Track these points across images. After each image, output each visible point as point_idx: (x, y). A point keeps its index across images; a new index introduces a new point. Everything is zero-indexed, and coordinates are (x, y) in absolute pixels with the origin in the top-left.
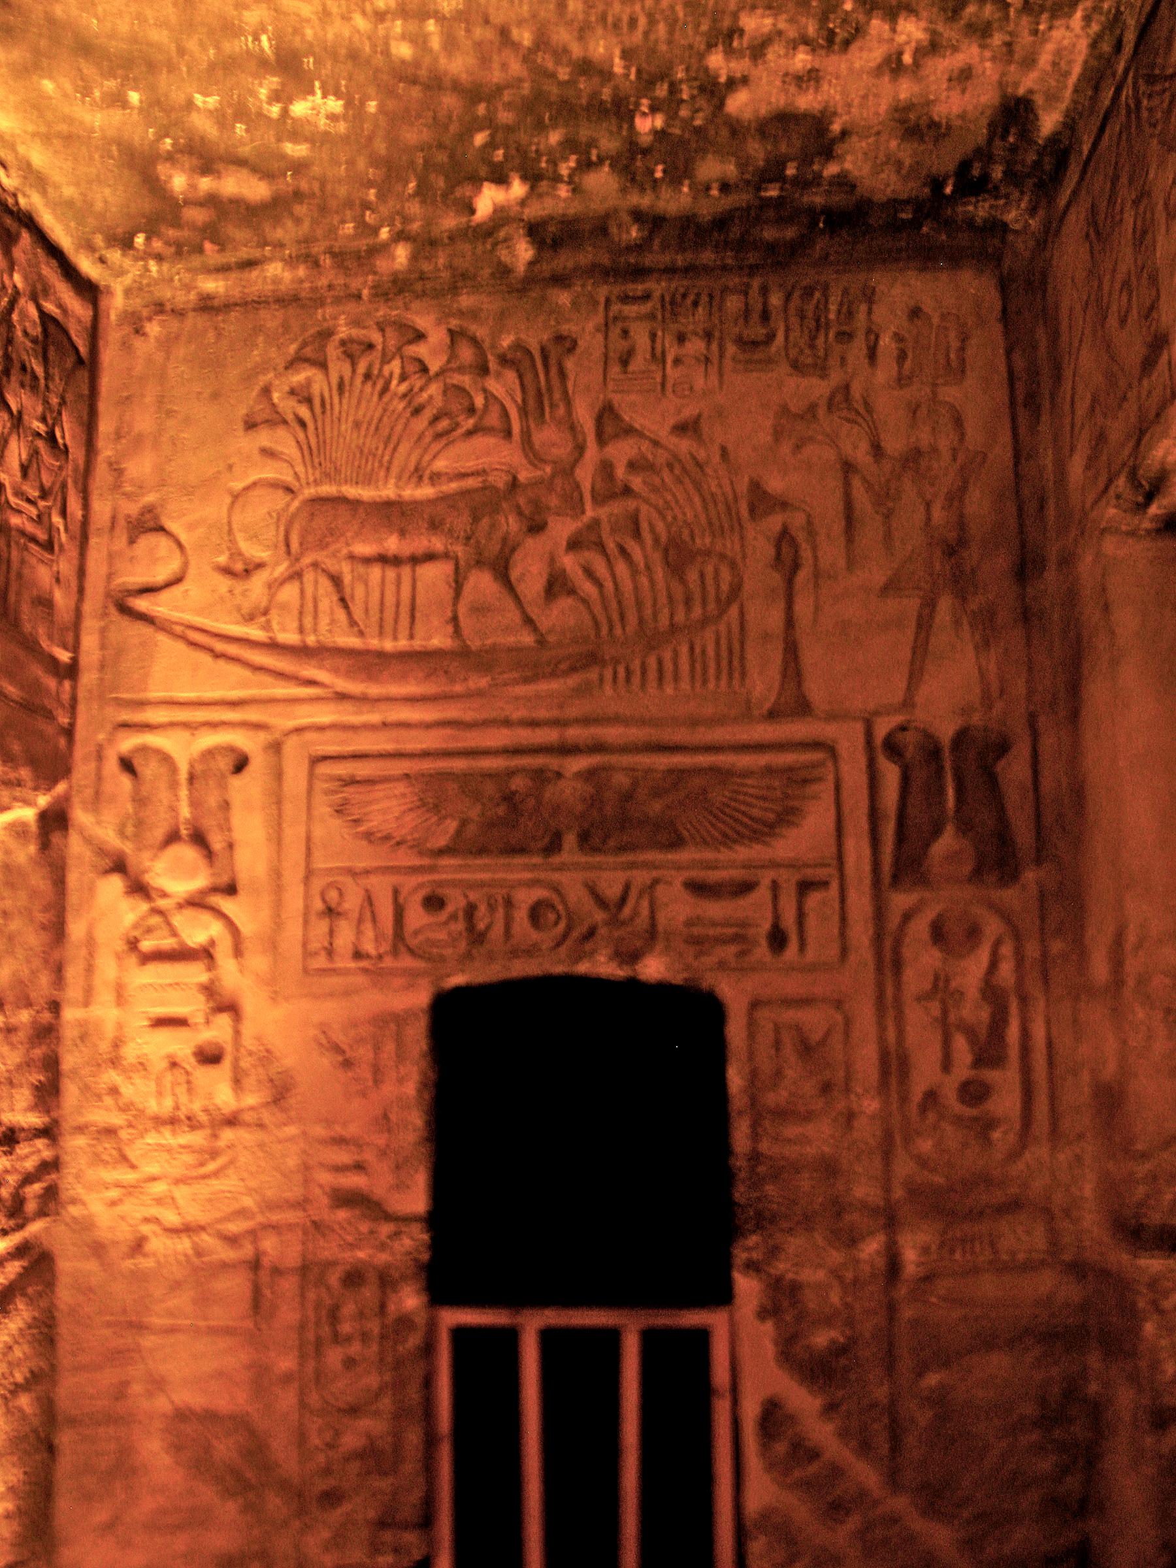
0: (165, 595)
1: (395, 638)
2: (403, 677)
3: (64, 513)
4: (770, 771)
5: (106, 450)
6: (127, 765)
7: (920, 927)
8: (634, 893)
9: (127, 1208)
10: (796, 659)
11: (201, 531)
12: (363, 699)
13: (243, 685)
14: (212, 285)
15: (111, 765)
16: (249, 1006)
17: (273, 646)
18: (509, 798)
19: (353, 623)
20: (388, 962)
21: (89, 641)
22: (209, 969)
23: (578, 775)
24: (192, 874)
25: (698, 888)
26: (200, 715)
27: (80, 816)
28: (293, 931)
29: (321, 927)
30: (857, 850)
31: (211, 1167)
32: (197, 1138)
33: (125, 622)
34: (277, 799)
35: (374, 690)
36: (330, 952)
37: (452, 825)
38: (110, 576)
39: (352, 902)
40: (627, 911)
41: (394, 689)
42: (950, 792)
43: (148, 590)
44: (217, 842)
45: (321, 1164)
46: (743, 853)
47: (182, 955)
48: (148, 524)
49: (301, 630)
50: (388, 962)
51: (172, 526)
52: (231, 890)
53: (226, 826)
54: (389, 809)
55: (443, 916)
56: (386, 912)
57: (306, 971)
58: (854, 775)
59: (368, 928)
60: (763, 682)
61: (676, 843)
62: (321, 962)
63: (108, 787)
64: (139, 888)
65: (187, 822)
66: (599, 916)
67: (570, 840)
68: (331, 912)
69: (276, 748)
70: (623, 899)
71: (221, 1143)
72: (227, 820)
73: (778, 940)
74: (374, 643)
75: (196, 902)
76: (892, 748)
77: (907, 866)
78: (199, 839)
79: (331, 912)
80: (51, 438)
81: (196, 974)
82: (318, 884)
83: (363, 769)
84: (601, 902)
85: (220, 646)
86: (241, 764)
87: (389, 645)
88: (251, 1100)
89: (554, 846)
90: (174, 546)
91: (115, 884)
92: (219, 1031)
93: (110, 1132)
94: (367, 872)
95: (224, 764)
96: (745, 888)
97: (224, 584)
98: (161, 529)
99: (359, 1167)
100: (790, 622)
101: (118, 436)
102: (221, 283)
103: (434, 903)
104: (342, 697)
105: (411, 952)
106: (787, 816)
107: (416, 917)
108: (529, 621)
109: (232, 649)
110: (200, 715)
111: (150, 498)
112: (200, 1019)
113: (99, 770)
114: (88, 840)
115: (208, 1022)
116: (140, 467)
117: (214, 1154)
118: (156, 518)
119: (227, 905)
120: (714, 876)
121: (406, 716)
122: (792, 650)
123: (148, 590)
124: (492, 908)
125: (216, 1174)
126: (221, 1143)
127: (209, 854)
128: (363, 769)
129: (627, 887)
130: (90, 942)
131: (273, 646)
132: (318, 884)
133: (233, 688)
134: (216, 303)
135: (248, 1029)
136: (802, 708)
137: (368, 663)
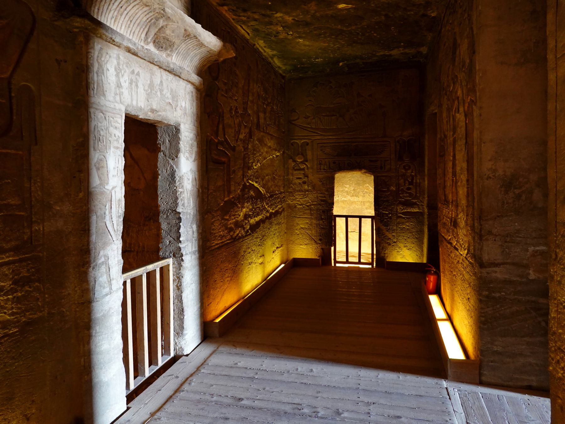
9: (294, 202)
16: (309, 176)
17: (312, 128)
26: (301, 138)
28: (316, 166)
32: (303, 193)
36: (320, 169)
47: (300, 169)
52: (307, 161)
64: (294, 161)
68: (320, 164)
73: (381, 168)
75: (302, 162)
78: (302, 154)
79: (320, 164)
83: (325, 145)
86: (308, 144)
91: (290, 161)
92: (306, 179)
93: (291, 192)
99: (325, 197)
103: (334, 163)
110: (301, 138)
127: (304, 157)
128: (325, 145)
130: (288, 168)
131: (312, 128)
135: (309, 179)
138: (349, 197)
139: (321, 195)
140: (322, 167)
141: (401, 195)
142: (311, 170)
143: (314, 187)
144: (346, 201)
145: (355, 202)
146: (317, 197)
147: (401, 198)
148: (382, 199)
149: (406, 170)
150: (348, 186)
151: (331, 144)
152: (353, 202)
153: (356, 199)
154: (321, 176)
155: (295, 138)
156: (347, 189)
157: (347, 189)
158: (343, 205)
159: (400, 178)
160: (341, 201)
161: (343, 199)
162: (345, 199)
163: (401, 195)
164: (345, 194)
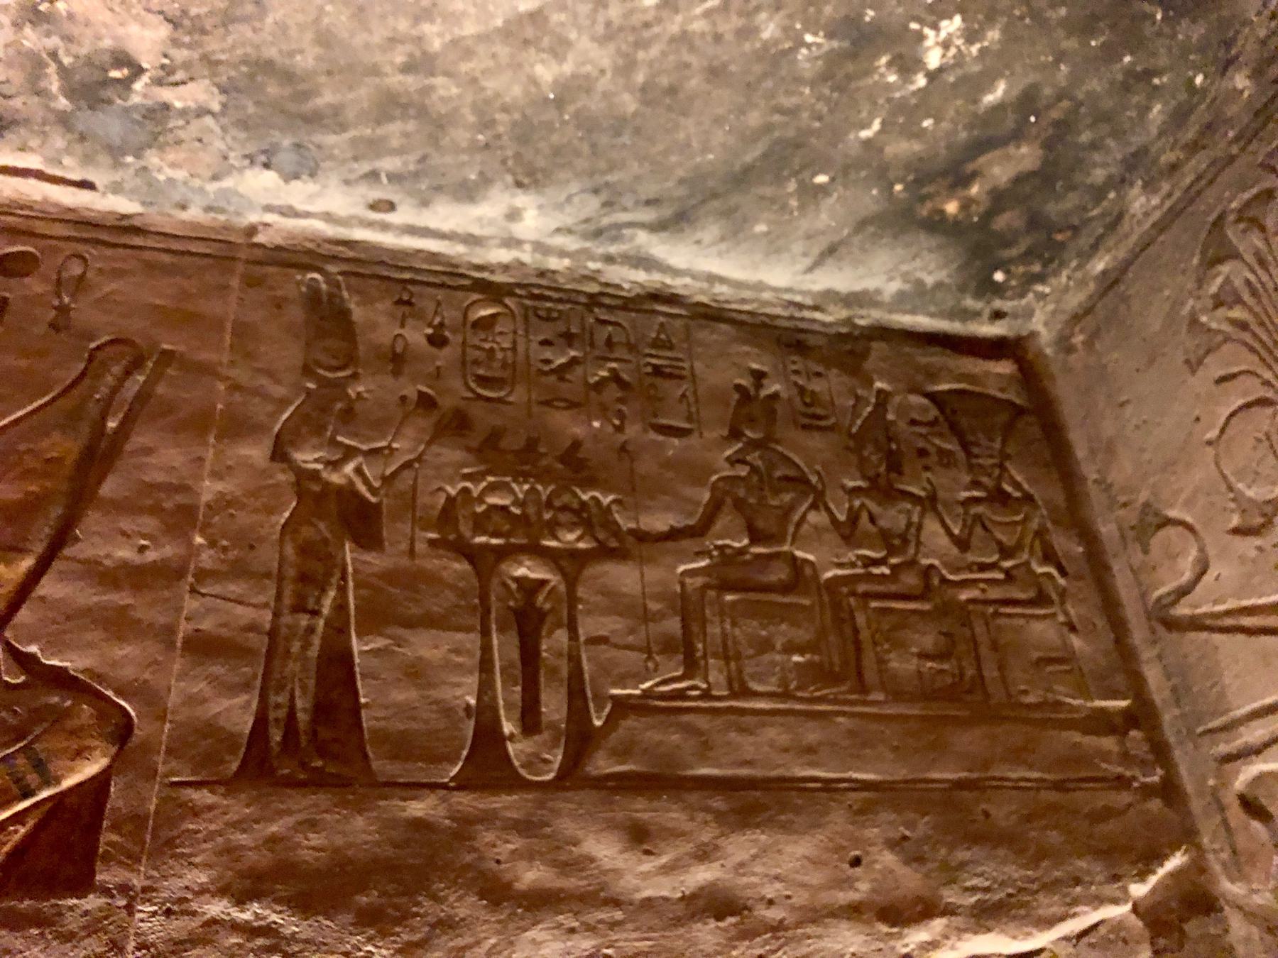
0: (1198, 588)
3: (1049, 556)
5: (1090, 472)
6: (1251, 806)
11: (1202, 500)
14: (1099, 265)
15: (1236, 814)
21: (1153, 675)
27: (1231, 888)
33: (1175, 636)
38: (1144, 595)
43: (1183, 592)
48: (1153, 522)
51: (1173, 513)
63: (1241, 842)
80: (999, 497)
90: (1186, 532)
97: (1248, 546)
98: (1169, 522)
101: (1093, 452)
102: (1107, 258)
111: (1143, 496)
113: (1225, 822)
114: (1251, 915)
116: (1122, 470)
118: (1156, 514)
123: (1183, 592)
134: (1113, 276)
155: (1256, 733)
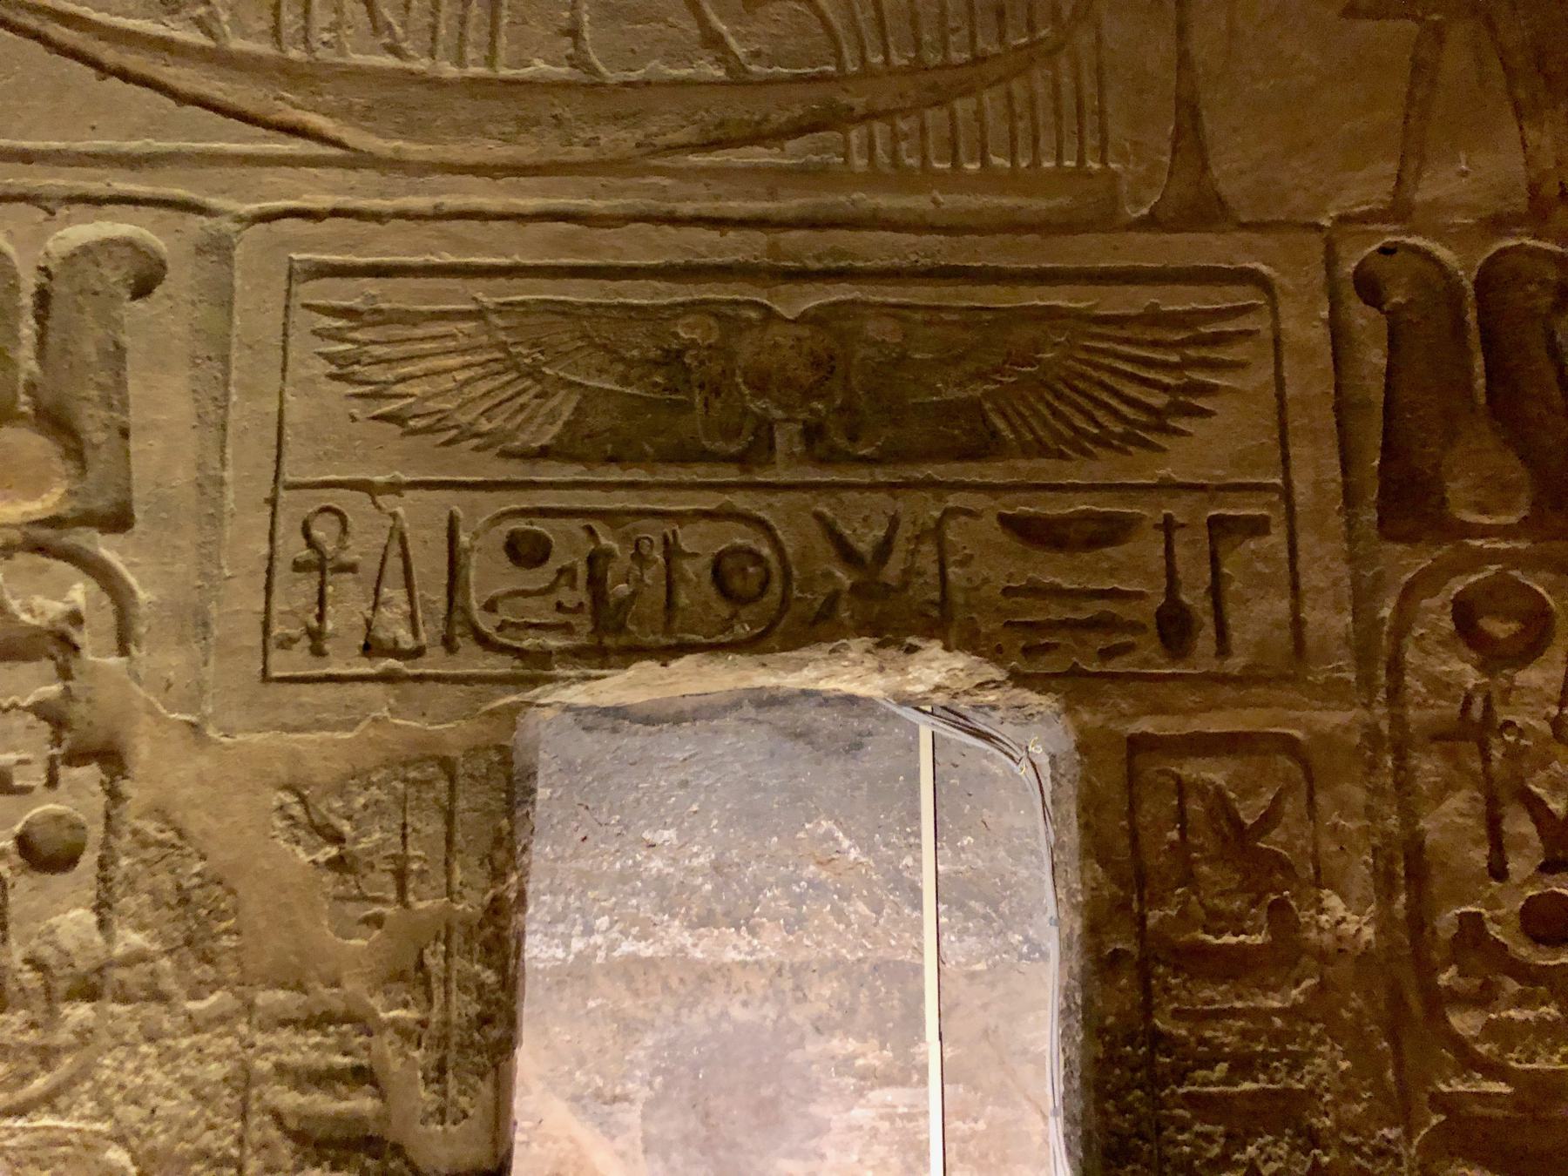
1: (460, 61)
2: (476, 128)
4: (1154, 318)
7: (1436, 613)
8: (905, 532)
10: (1196, 127)
12: (396, 164)
13: (155, 127)
16: (142, 750)
18: (672, 358)
19: (377, 26)
20: (434, 662)
22: (65, 674)
23: (802, 319)
24: (36, 488)
25: (1026, 530)
29: (296, 594)
30: (1315, 469)
31: (40, 1084)
34: (215, 350)
35: (415, 150)
36: (316, 640)
37: (565, 405)
39: (363, 546)
40: (892, 570)
41: (457, 152)
42: (1479, 364)
44: (93, 424)
45: (280, 1068)
46: (1105, 466)
49: (276, 33)
50: (434, 662)
52: (118, 521)
53: (115, 396)
54: (444, 375)
55: (542, 576)
56: (430, 564)
57: (265, 677)
58: (1306, 327)
59: (394, 592)
60: (1139, 170)
61: (984, 447)
62: (294, 661)
65: (31, 387)
66: (844, 578)
67: (786, 438)
68: (319, 565)
69: (219, 248)
70: (884, 549)
71: (63, 1036)
72: (121, 384)
73: (1174, 627)
74: (422, 64)
76: (1369, 287)
77: (1406, 500)
78: (56, 422)
81: (37, 683)
82: (294, 507)
84: (848, 555)
85: (109, 54)
86: (146, 280)
87: (449, 71)
88: (131, 939)
89: (759, 450)
94: (395, 488)
95: (114, 276)
96: (1112, 530)
99: (361, 1076)
100: (1184, 61)
103: (525, 551)
104: (357, 160)
105: (483, 640)
106: (1189, 401)
107: (490, 575)
108: (714, 41)
109: (135, 61)
112: (35, 776)
115: (52, 782)
117: (47, 1056)
119: (107, 548)
120: (1053, 507)
121: (477, 206)
122: (1189, 111)
124: (639, 557)
125: (48, 1100)
126: (63, 1036)
129: (894, 523)
132: (294, 507)
133: (131, 137)
136: (1204, 211)
137: (404, 98)
138: (677, 934)
139: (305, 1049)
140: (347, 610)
141: (1464, 1022)
142: (163, 658)
143: (196, 920)
144: (651, 963)
145: (724, 970)
146: (244, 1080)
147: (1469, 1062)
148: (1213, 1080)
149: (1492, 656)
150: (669, 835)
151: (485, 293)
152: (707, 977)
153: (733, 947)
154: (320, 751)
156: (656, 864)
157: (656, 864)
158: (627, 1003)
159: (1428, 767)
160: (609, 969)
161: (627, 947)
162: (646, 950)
163: (1464, 1022)
164: (644, 906)
